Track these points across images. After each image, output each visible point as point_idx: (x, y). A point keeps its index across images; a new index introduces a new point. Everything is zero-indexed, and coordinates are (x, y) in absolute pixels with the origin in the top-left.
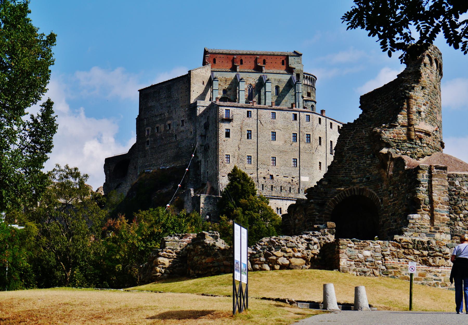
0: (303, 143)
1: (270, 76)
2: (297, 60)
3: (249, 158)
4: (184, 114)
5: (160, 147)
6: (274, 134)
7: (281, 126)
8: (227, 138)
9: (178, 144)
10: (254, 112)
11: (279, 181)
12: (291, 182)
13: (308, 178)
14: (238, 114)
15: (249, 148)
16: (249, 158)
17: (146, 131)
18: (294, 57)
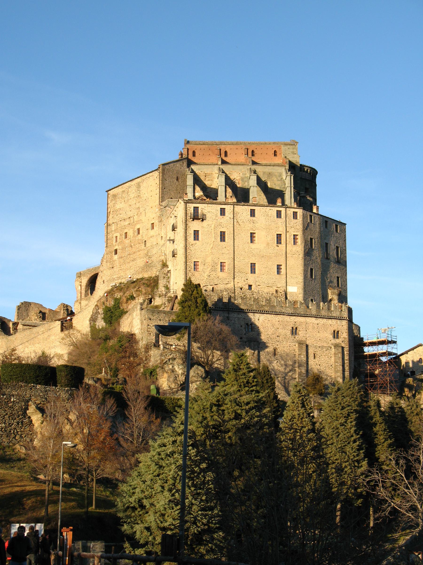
0: (290, 245)
1: (259, 169)
2: (292, 150)
3: (222, 265)
4: (154, 215)
5: (129, 256)
6: (252, 235)
7: (262, 226)
8: (197, 241)
9: (148, 252)
10: (228, 209)
11: (260, 292)
12: (275, 293)
13: (296, 288)
14: (209, 212)
15: (224, 253)
16: (222, 265)
17: (114, 238)
18: (289, 147)
